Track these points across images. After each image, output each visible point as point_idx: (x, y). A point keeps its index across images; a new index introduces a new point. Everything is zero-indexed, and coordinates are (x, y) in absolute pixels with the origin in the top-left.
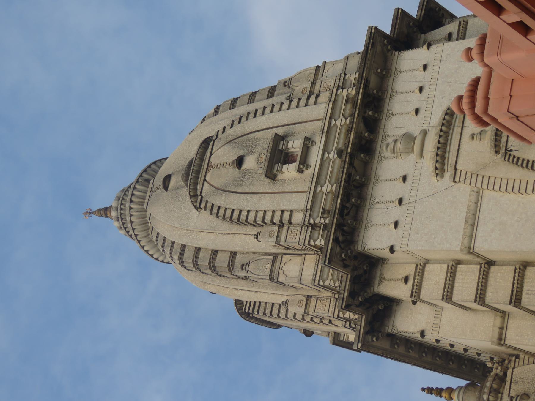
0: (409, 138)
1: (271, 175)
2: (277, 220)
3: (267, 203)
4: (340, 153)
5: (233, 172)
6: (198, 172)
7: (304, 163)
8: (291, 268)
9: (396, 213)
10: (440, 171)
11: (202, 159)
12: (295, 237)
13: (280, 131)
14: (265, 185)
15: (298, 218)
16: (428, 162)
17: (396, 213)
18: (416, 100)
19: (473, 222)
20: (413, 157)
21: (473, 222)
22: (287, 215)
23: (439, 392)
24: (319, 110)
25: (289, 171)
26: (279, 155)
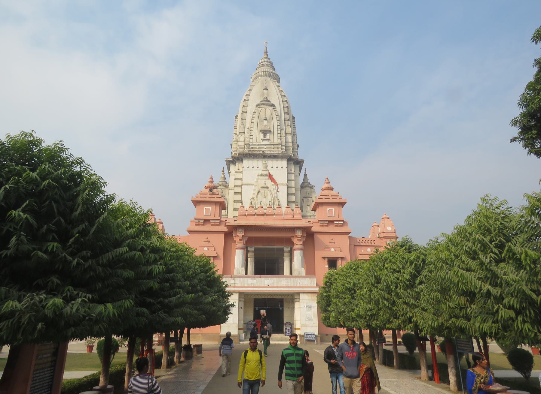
0: (266, 167)
1: (261, 131)
2: (251, 134)
4: (263, 151)
5: (263, 117)
6: (264, 105)
7: (263, 140)
8: (242, 138)
9: (251, 167)
10: (258, 176)
11: (268, 105)
12: (247, 141)
13: (272, 131)
14: (259, 130)
15: (251, 141)
18: (275, 167)
19: (248, 184)
21: (248, 184)
22: (251, 137)
23: (223, 171)
25: (262, 136)
26: (265, 132)
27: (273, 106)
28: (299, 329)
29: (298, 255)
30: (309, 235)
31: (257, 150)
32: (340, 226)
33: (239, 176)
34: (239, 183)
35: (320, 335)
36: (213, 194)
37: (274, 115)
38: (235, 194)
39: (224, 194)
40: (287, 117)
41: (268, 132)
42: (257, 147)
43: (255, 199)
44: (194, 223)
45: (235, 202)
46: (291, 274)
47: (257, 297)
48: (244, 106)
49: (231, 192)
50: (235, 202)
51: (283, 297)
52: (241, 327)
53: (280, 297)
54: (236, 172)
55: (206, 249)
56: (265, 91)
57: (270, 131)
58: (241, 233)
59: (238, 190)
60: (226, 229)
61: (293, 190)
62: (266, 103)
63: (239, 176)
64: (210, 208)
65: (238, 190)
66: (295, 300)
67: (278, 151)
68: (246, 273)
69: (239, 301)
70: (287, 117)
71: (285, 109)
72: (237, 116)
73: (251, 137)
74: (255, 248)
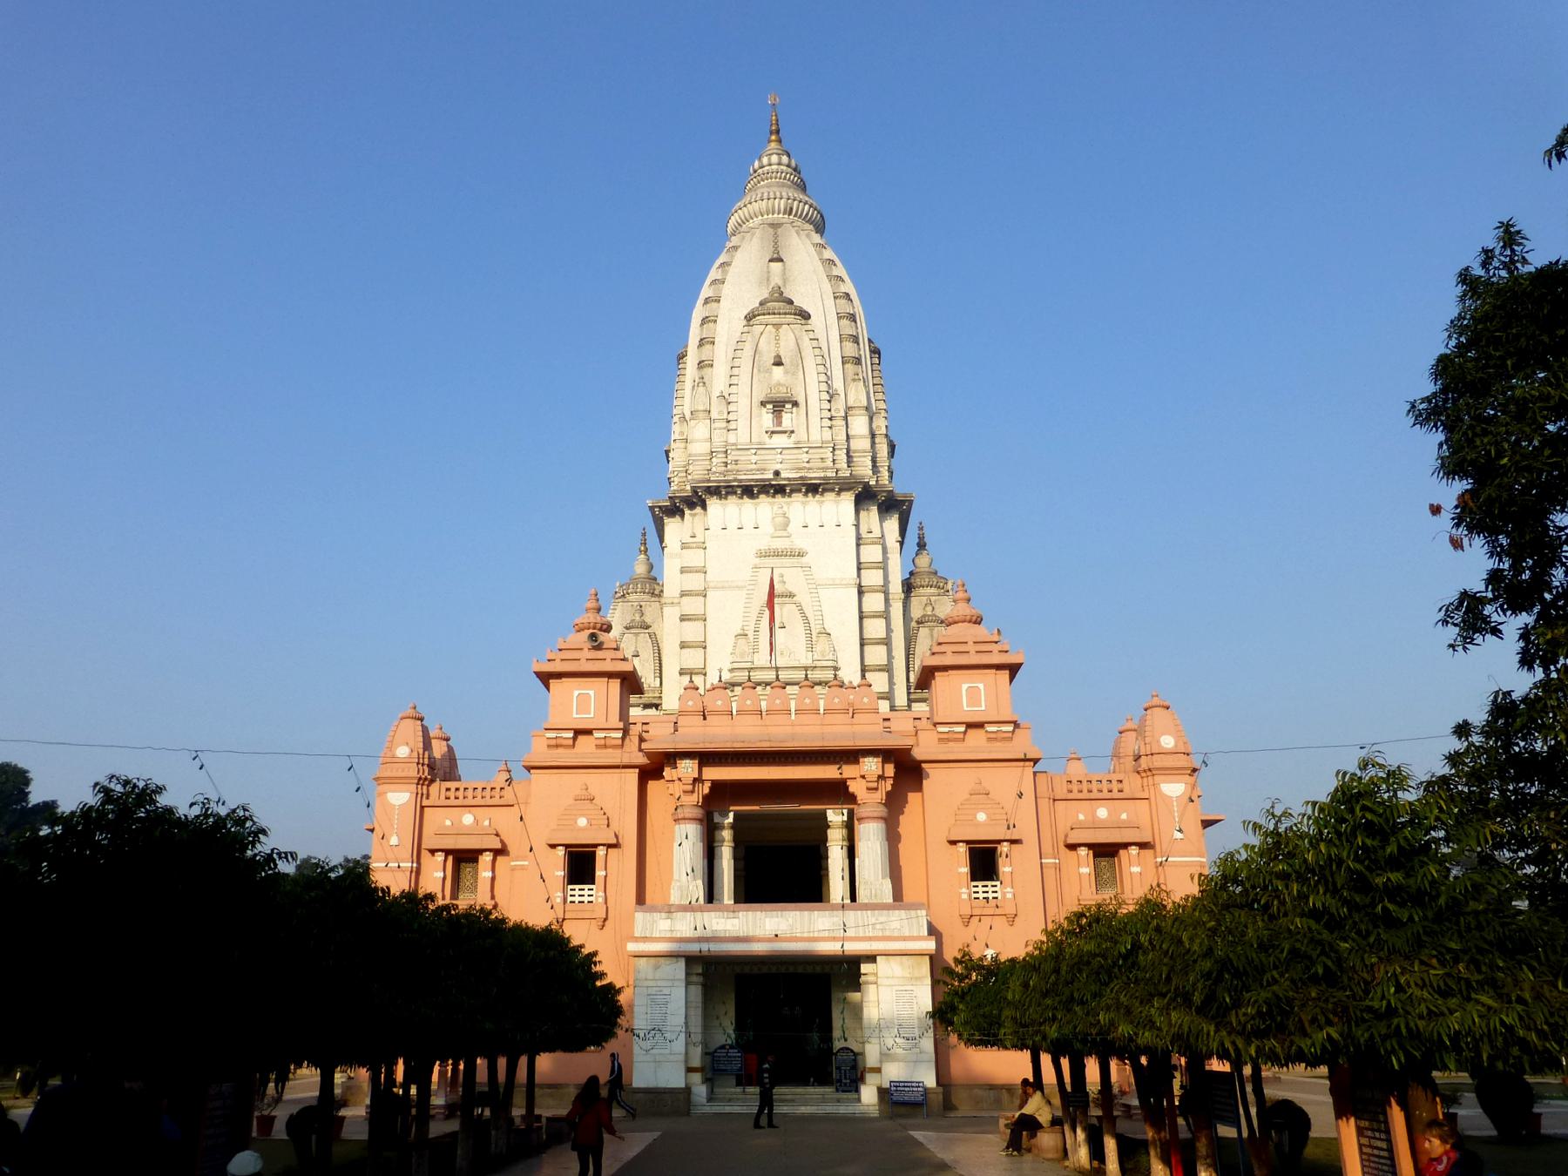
1: (763, 404)
3: (742, 405)
9: (732, 526)
12: (719, 438)
14: (757, 399)
15: (732, 438)
16: (766, 543)
17: (732, 526)
18: (813, 525)
20: (771, 530)
24: (816, 436)
25: (767, 418)
26: (778, 405)
27: (805, 316)
28: (878, 1070)
29: (871, 839)
30: (907, 770)
31: (751, 468)
32: (1004, 739)
33: (694, 558)
34: (694, 582)
35: (941, 1089)
36: (599, 647)
37: (807, 344)
38: (684, 618)
39: (648, 620)
40: (850, 349)
41: (788, 406)
42: (754, 459)
43: (751, 634)
44: (546, 742)
45: (683, 645)
46: (853, 898)
47: (747, 970)
48: (705, 321)
49: (671, 614)
50: (683, 645)
51: (827, 969)
52: (696, 1063)
53: (818, 969)
54: (684, 546)
55: (582, 822)
56: (776, 266)
57: (795, 404)
58: (688, 768)
59: (692, 606)
60: (641, 760)
61: (874, 602)
62: (781, 306)
63: (694, 558)
64: (592, 693)
65: (692, 606)
66: (863, 979)
67: (825, 469)
68: (711, 896)
69: (688, 983)
70: (850, 349)
71: (845, 322)
72: (682, 357)
73: (732, 425)
74: (737, 816)
